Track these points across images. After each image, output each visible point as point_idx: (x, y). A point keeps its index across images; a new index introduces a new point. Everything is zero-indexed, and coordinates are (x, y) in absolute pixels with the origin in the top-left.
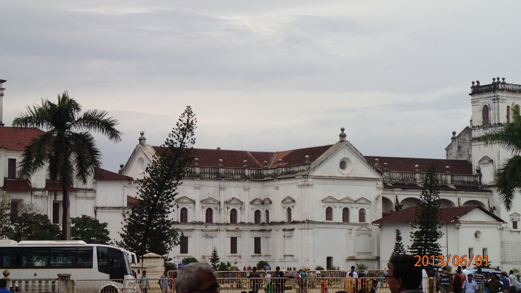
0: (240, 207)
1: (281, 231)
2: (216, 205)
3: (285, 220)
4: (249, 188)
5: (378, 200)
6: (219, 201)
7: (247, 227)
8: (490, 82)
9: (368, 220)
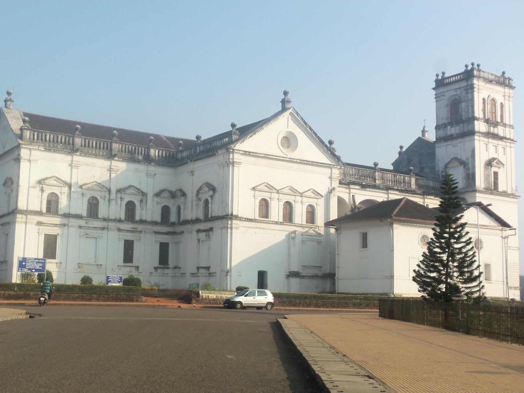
0: (140, 199)
1: (195, 233)
2: (103, 193)
3: (201, 216)
4: (155, 174)
5: (332, 195)
6: (109, 188)
7: (149, 227)
8: (463, 70)
9: (320, 220)
